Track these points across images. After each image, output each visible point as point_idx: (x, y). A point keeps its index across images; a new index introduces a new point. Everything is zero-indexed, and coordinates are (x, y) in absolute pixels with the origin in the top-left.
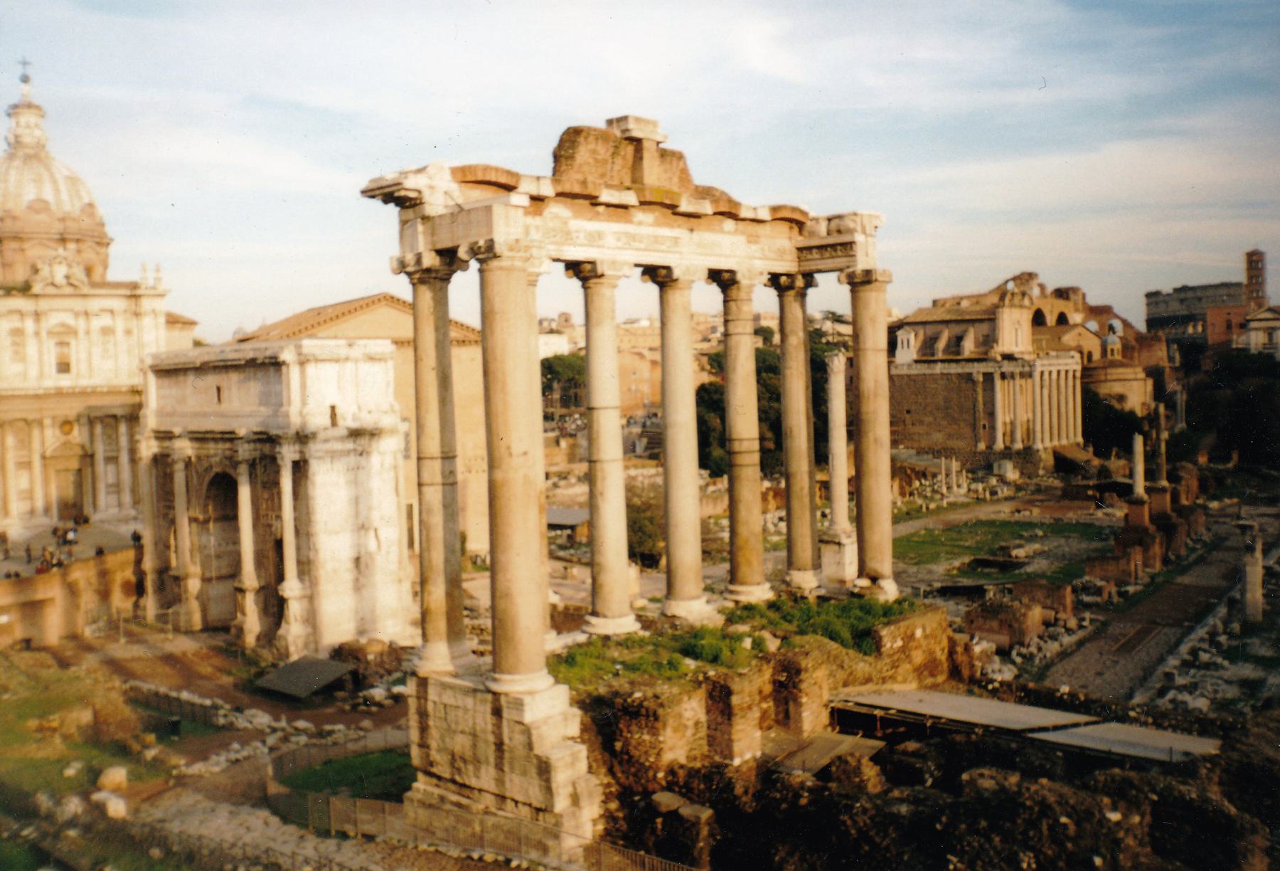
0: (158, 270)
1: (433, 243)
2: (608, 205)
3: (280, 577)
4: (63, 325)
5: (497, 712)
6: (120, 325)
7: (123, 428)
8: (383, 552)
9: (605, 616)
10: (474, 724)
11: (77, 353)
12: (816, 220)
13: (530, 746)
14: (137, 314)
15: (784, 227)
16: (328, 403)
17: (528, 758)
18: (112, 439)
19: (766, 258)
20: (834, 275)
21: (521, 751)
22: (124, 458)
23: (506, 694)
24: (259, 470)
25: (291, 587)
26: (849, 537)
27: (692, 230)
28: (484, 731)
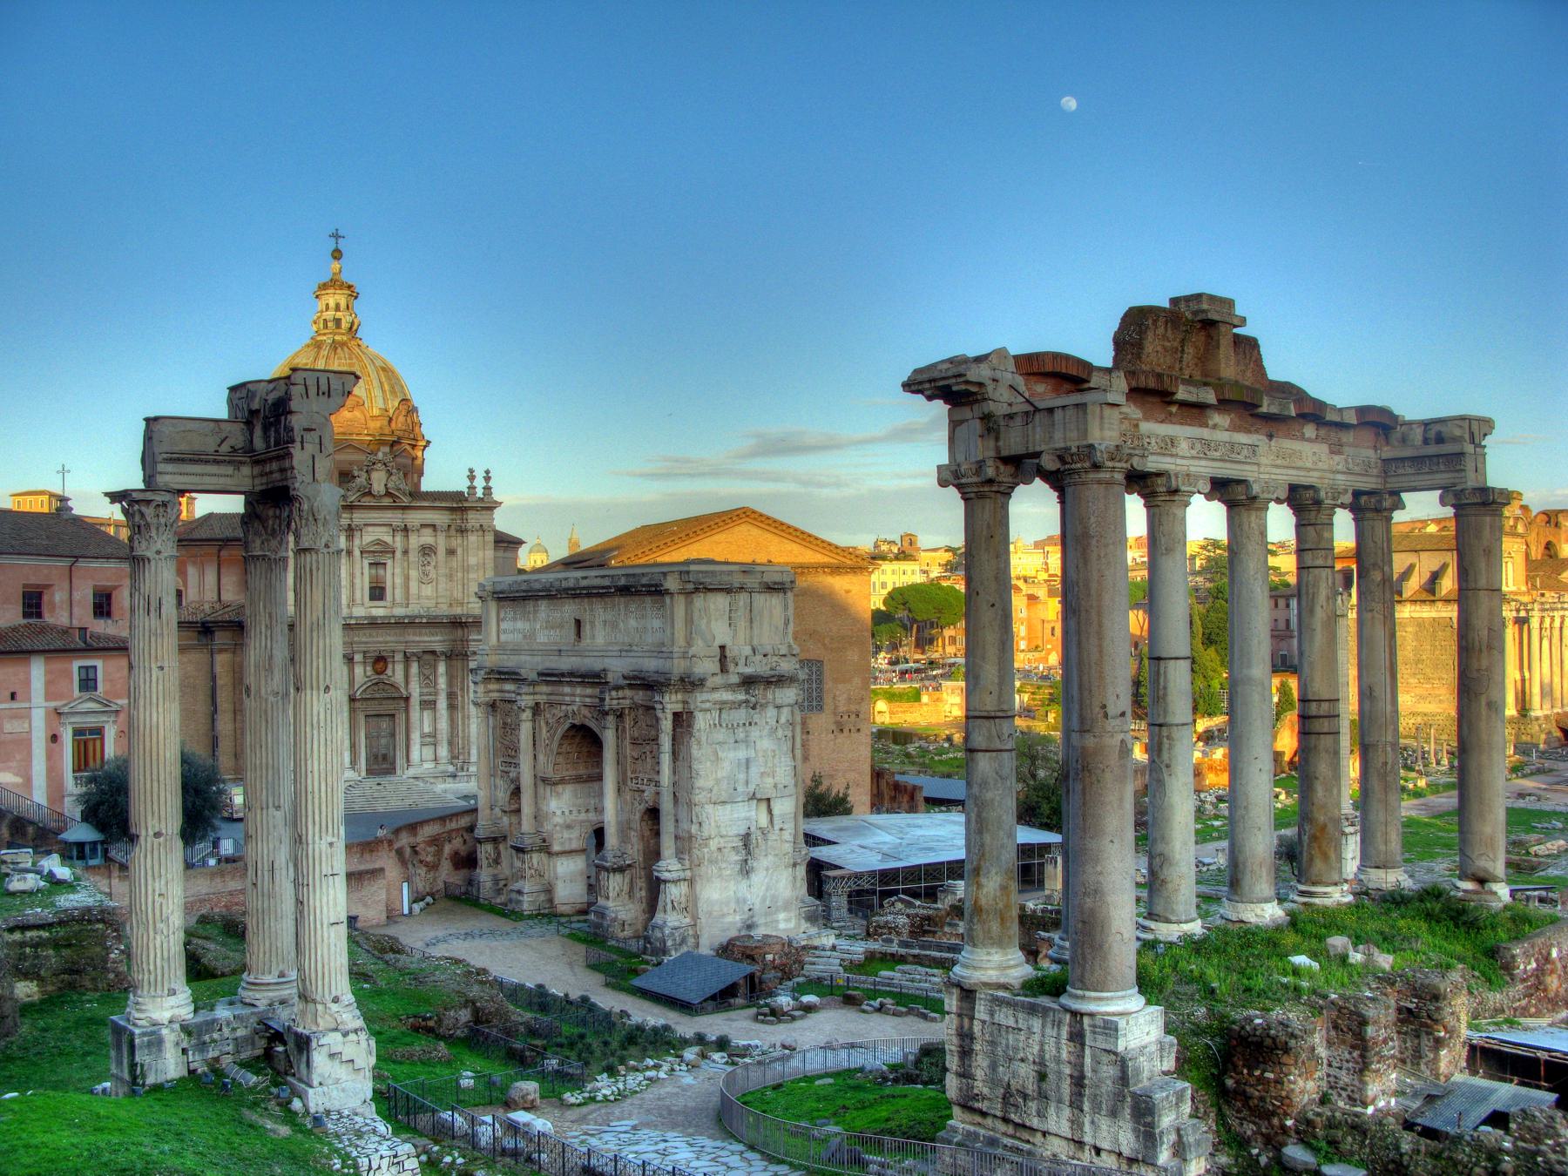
0: (487, 479)
1: (998, 450)
2: (1184, 404)
3: (654, 855)
4: (379, 542)
5: (1077, 1037)
6: (441, 543)
7: (442, 668)
8: (777, 827)
9: (1168, 921)
10: (1042, 1050)
11: (393, 575)
12: (1410, 423)
13: (1124, 1079)
14: (462, 531)
15: (1367, 435)
16: (718, 643)
17: (1119, 1097)
18: (429, 679)
19: (1349, 472)
20: (1438, 493)
21: (1108, 1087)
22: (442, 704)
23: (1091, 1015)
24: (628, 722)
25: (669, 866)
26: (1352, 825)
27: (1270, 437)
28: (1058, 1060)
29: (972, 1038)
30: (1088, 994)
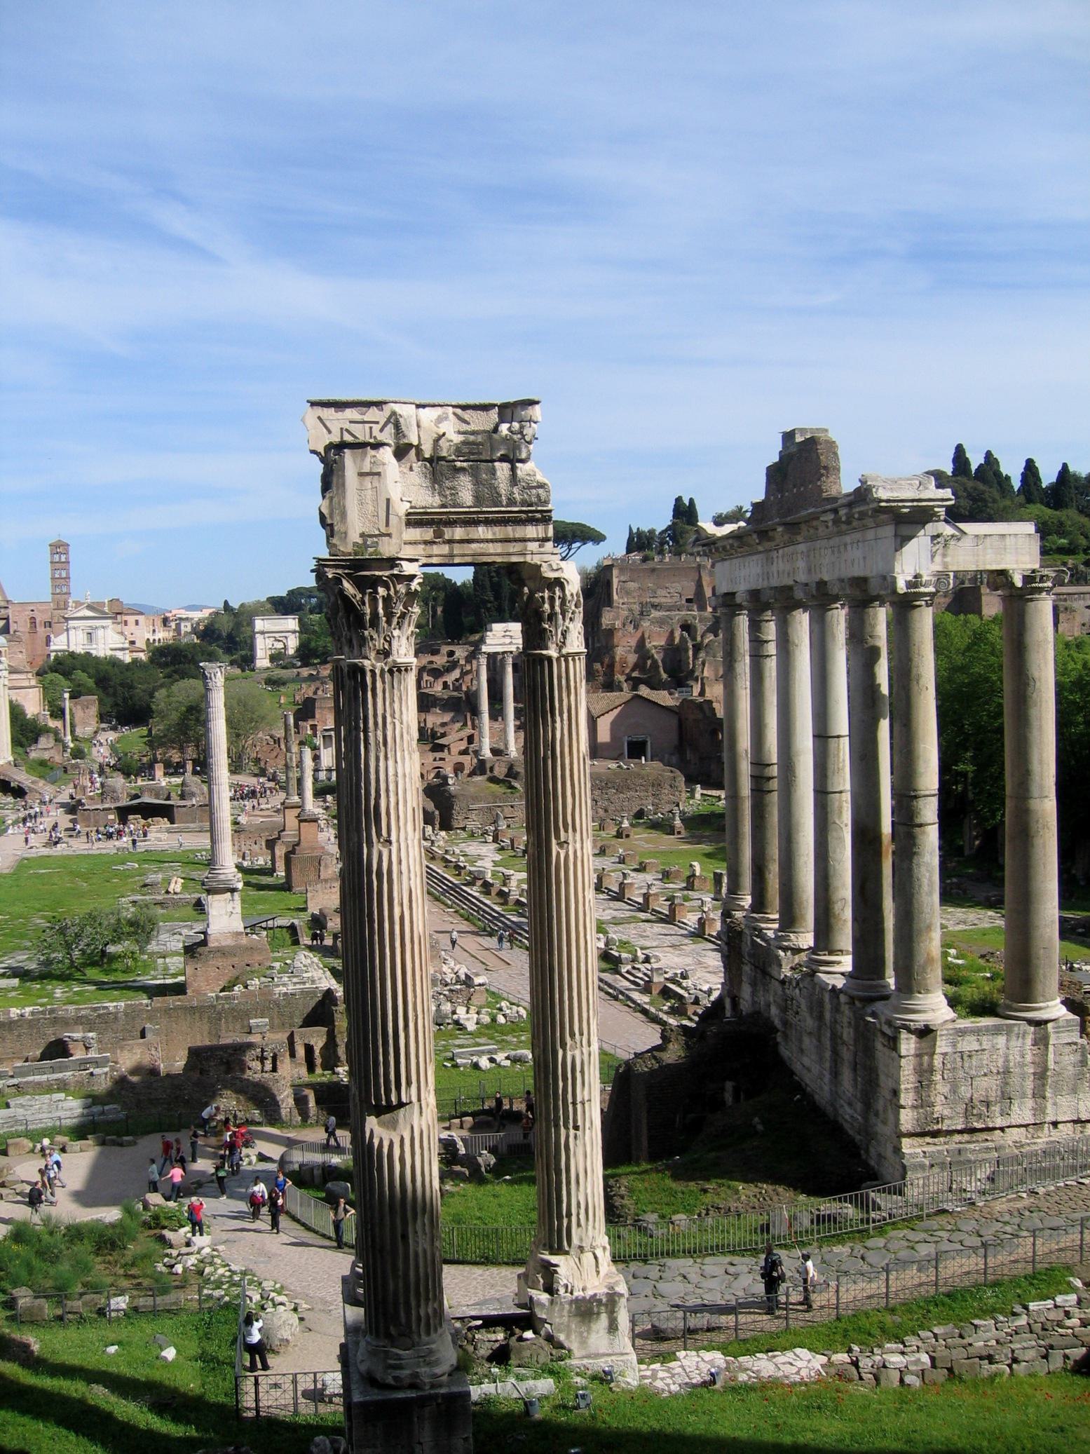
10: (1007, 1061)
28: (1022, 1065)
29: (931, 1070)
30: (1050, 1003)
